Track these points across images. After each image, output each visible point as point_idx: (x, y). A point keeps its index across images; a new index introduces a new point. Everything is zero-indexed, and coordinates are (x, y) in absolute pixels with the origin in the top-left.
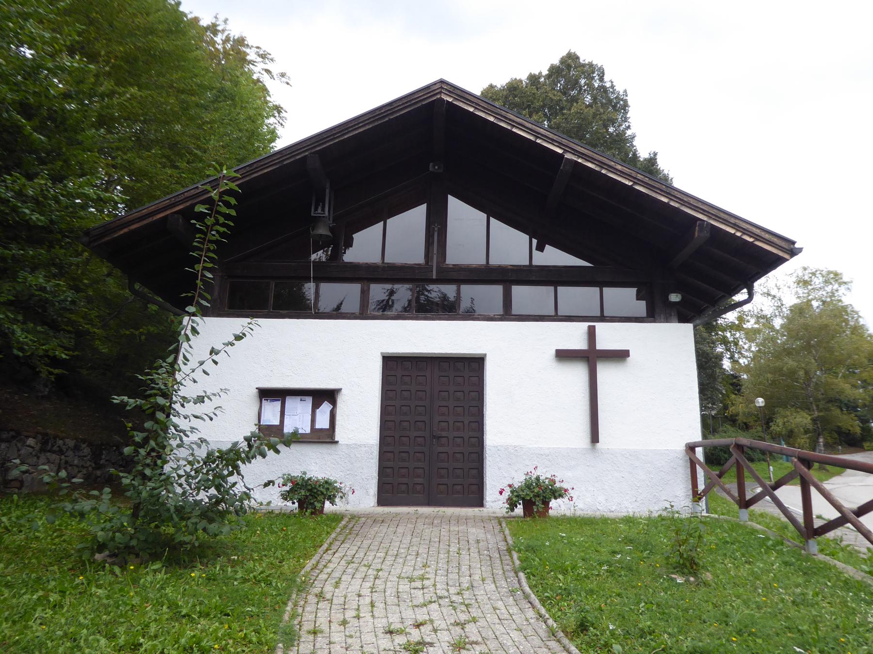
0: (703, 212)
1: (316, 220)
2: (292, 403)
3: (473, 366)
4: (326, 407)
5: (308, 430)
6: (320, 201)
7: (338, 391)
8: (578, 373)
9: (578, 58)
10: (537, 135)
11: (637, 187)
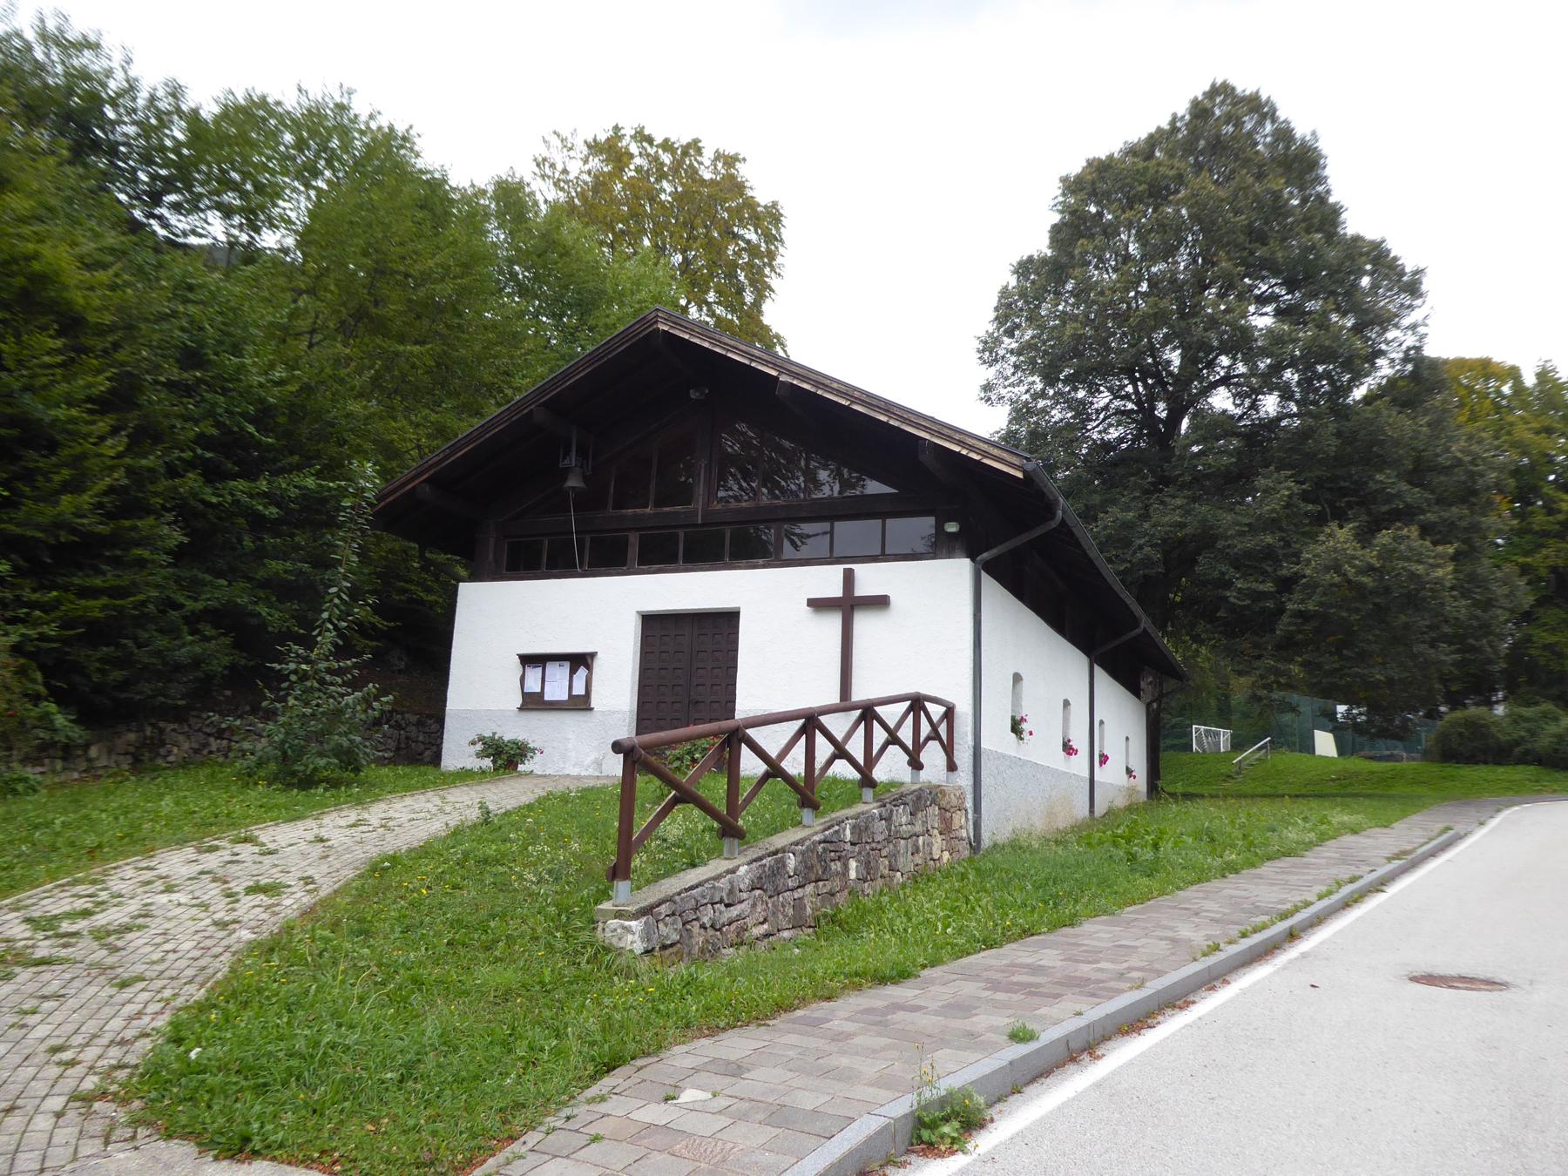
0: (926, 429)
1: (567, 470)
2: (552, 668)
3: (727, 621)
4: (582, 672)
5: (565, 697)
6: (567, 453)
7: (593, 655)
8: (832, 624)
9: (1233, 89)
10: (752, 357)
11: (855, 407)
